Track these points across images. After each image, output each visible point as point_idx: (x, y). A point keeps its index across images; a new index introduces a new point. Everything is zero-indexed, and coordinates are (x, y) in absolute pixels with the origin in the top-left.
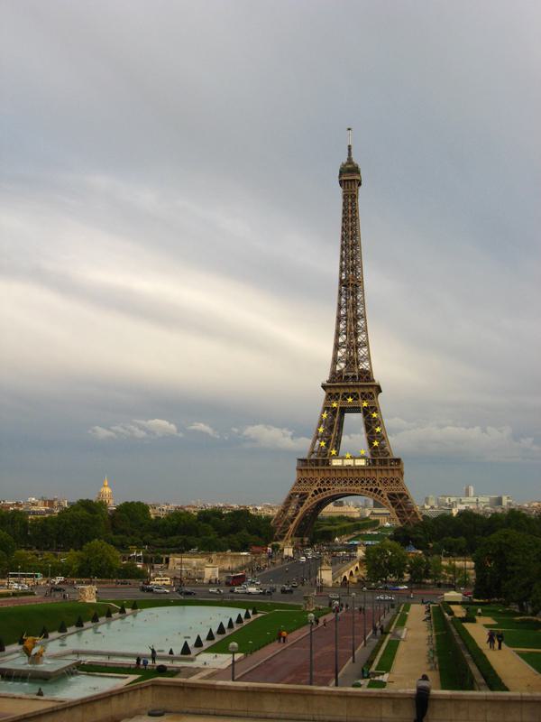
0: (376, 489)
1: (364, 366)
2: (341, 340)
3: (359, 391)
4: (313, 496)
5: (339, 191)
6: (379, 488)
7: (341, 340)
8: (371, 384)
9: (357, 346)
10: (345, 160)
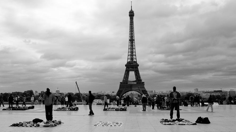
0: (139, 89)
1: (134, 60)
2: (129, 54)
3: (134, 66)
4: (124, 91)
5: (129, 17)
6: (140, 89)
7: (129, 54)
8: (137, 64)
9: (133, 56)
10: (130, 10)
